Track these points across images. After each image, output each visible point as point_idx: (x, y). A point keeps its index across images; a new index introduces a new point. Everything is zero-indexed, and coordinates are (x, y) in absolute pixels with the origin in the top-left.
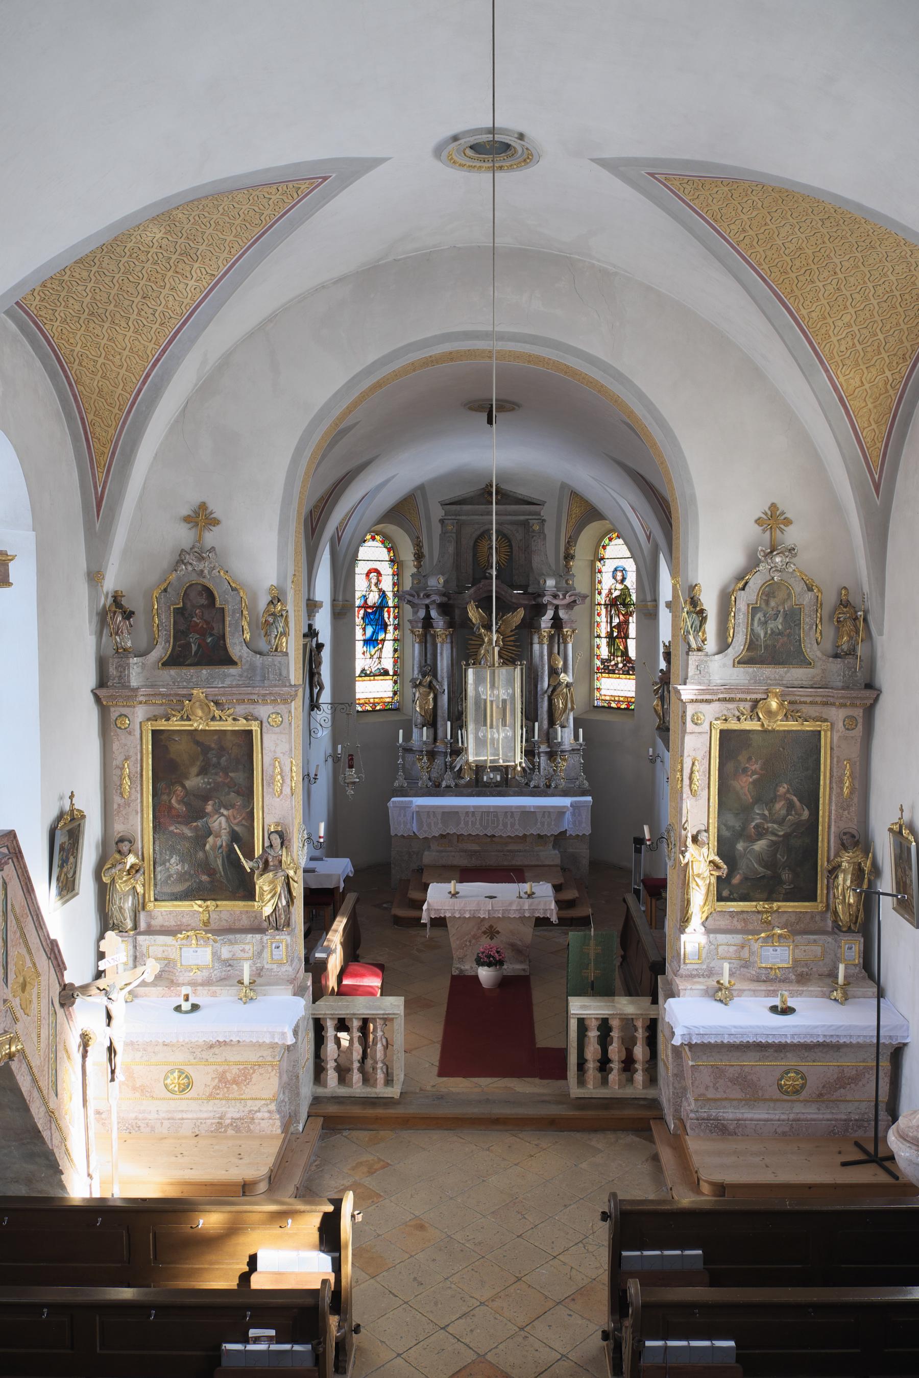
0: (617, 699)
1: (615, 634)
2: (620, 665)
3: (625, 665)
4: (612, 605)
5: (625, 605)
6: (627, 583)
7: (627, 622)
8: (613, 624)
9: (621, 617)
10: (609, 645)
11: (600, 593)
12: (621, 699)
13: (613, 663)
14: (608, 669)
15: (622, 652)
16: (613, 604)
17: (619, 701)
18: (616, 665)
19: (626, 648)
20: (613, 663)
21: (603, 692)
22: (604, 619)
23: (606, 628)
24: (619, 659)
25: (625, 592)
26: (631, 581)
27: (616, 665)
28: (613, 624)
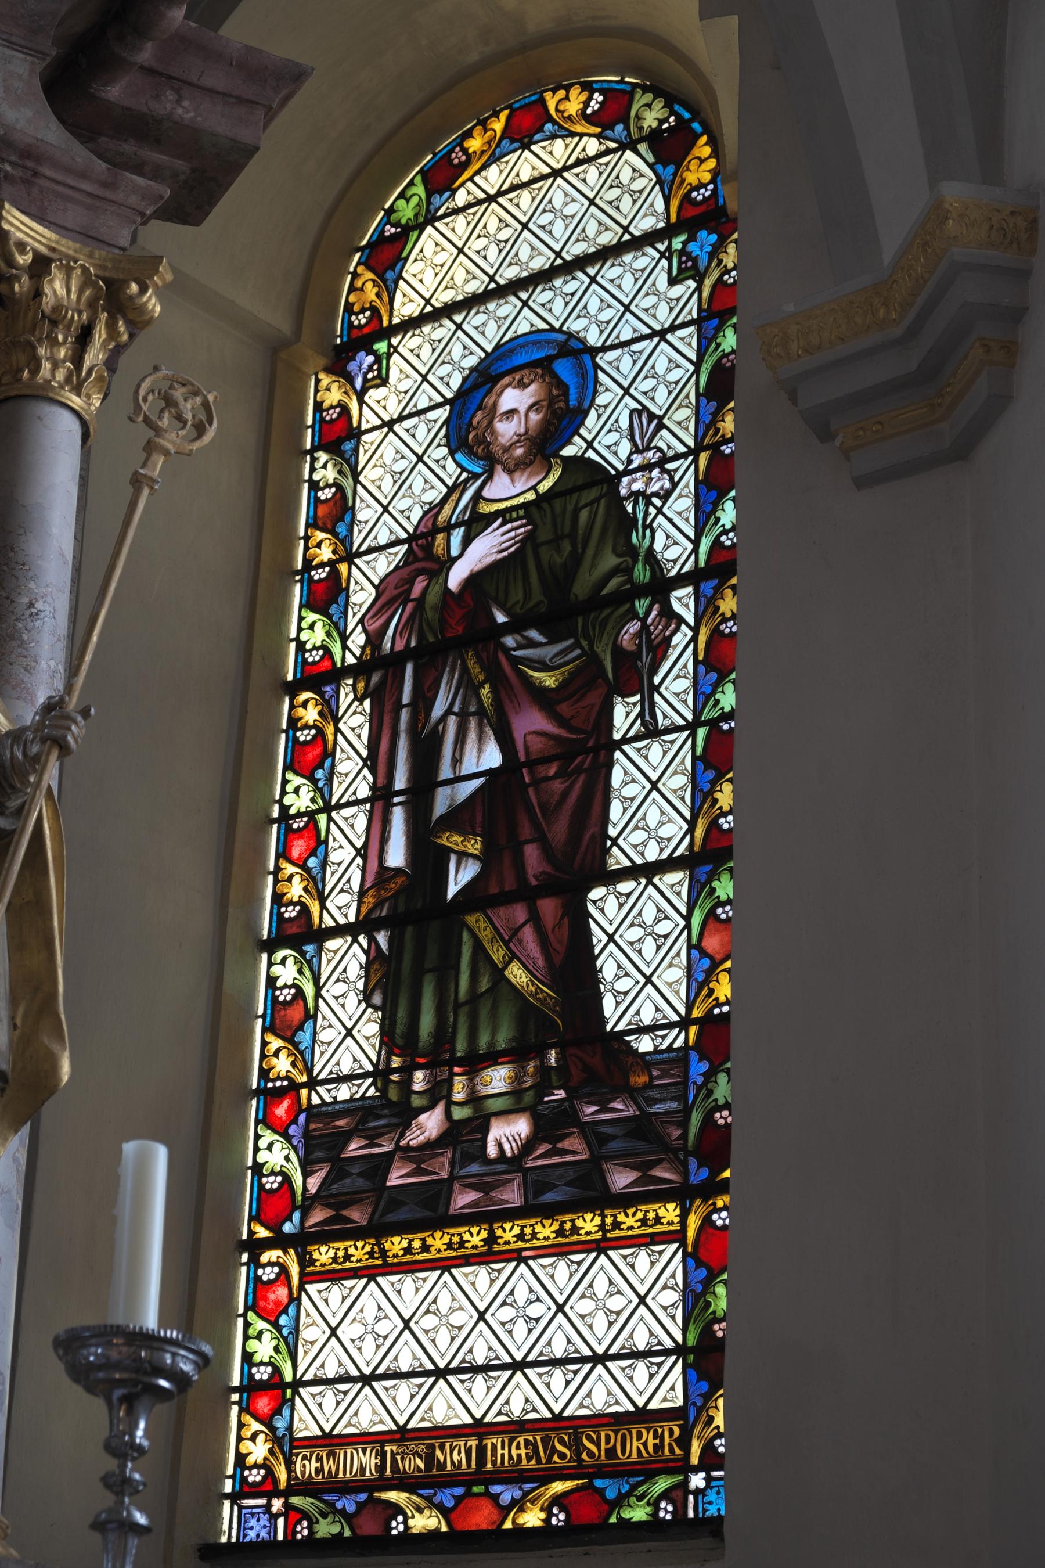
0: (455, 1456)
1: (459, 878)
2: (508, 1133)
3: (548, 1128)
4: (429, 657)
5: (559, 616)
6: (604, 437)
7: (592, 754)
8: (442, 802)
9: (530, 723)
10: (384, 983)
11: (326, 597)
12: (503, 1452)
13: (430, 1124)
14: (380, 1198)
15: (525, 1009)
16: (438, 637)
17: (479, 1478)
18: (465, 1136)
19: (575, 968)
20: (430, 1124)
21: (313, 1414)
22: (351, 774)
23: (371, 850)
24: (497, 1079)
25: (587, 508)
26: (648, 386)
27: (465, 1136)
28: (442, 802)
